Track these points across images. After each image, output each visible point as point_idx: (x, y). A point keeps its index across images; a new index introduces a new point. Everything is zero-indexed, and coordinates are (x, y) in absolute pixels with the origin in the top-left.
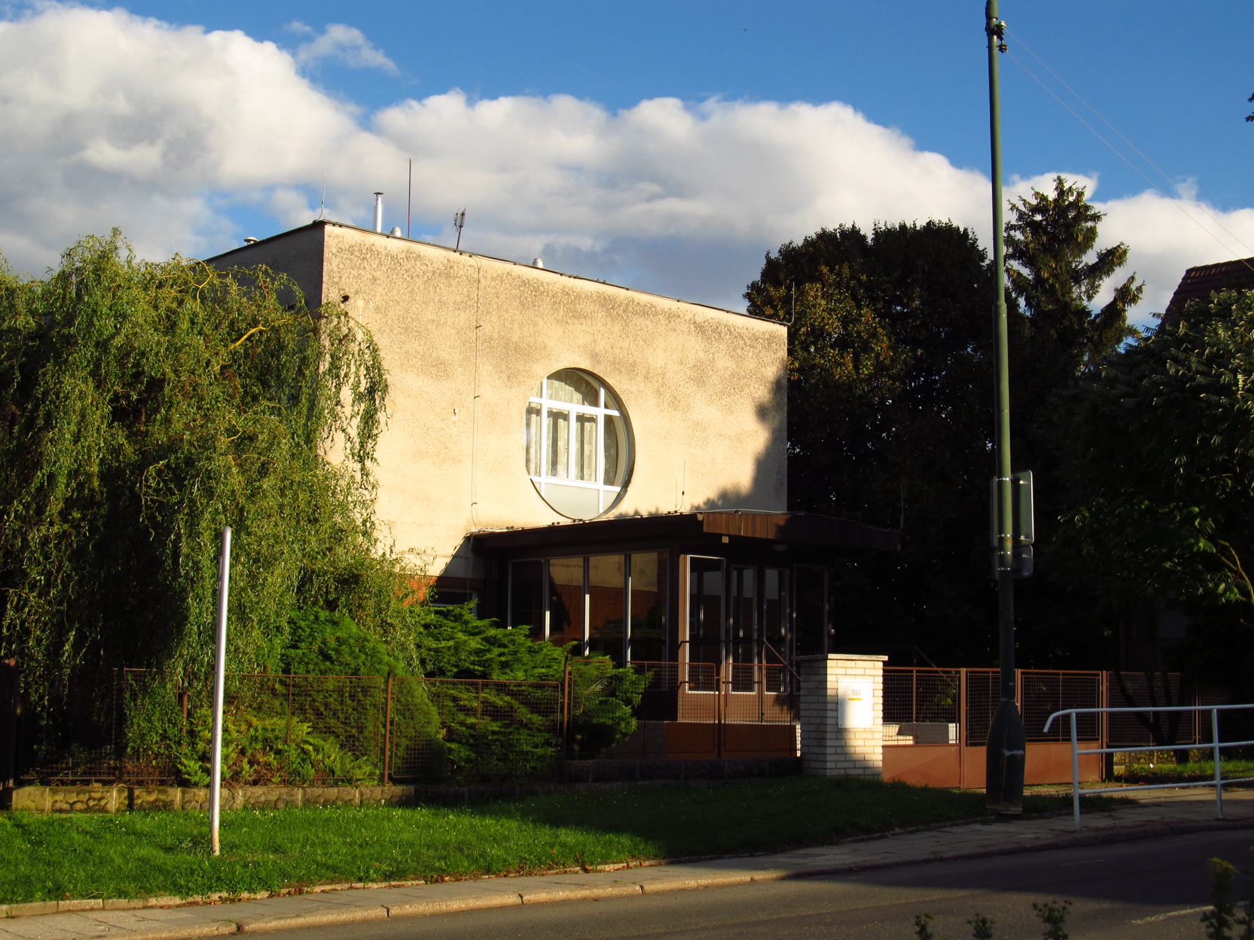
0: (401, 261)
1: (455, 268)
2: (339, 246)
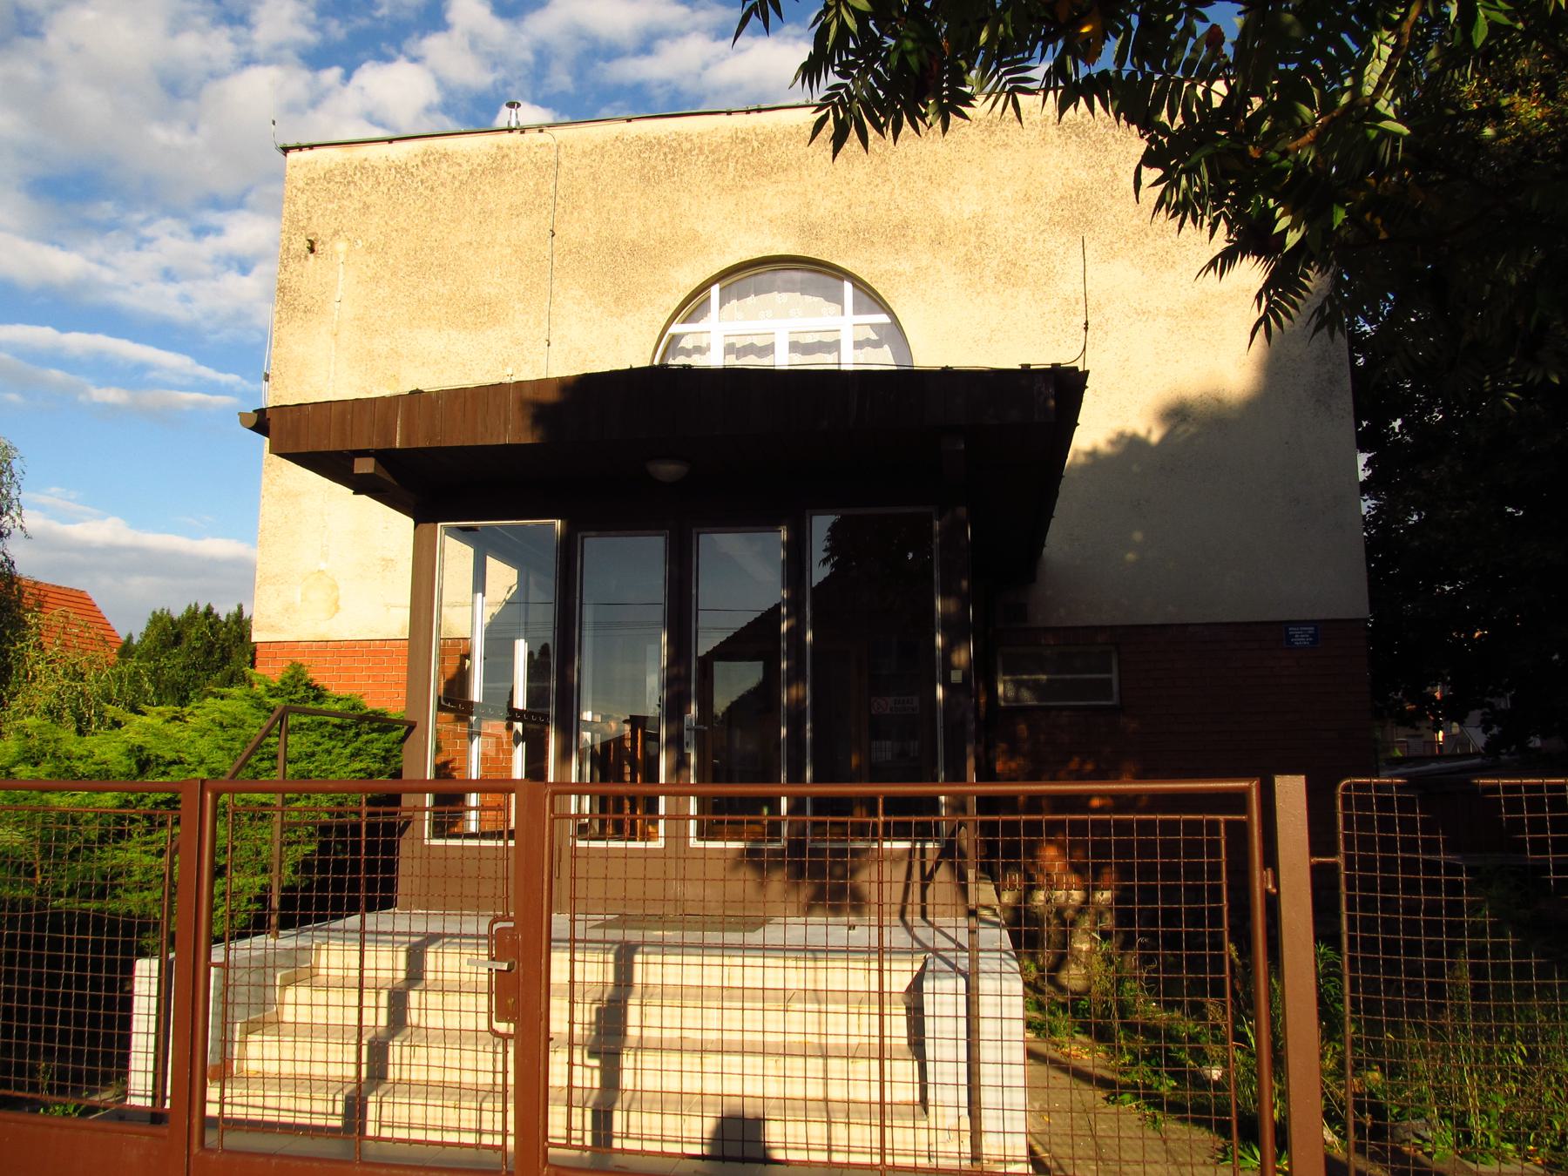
0: (414, 170)
1: (512, 155)
2: (309, 176)
